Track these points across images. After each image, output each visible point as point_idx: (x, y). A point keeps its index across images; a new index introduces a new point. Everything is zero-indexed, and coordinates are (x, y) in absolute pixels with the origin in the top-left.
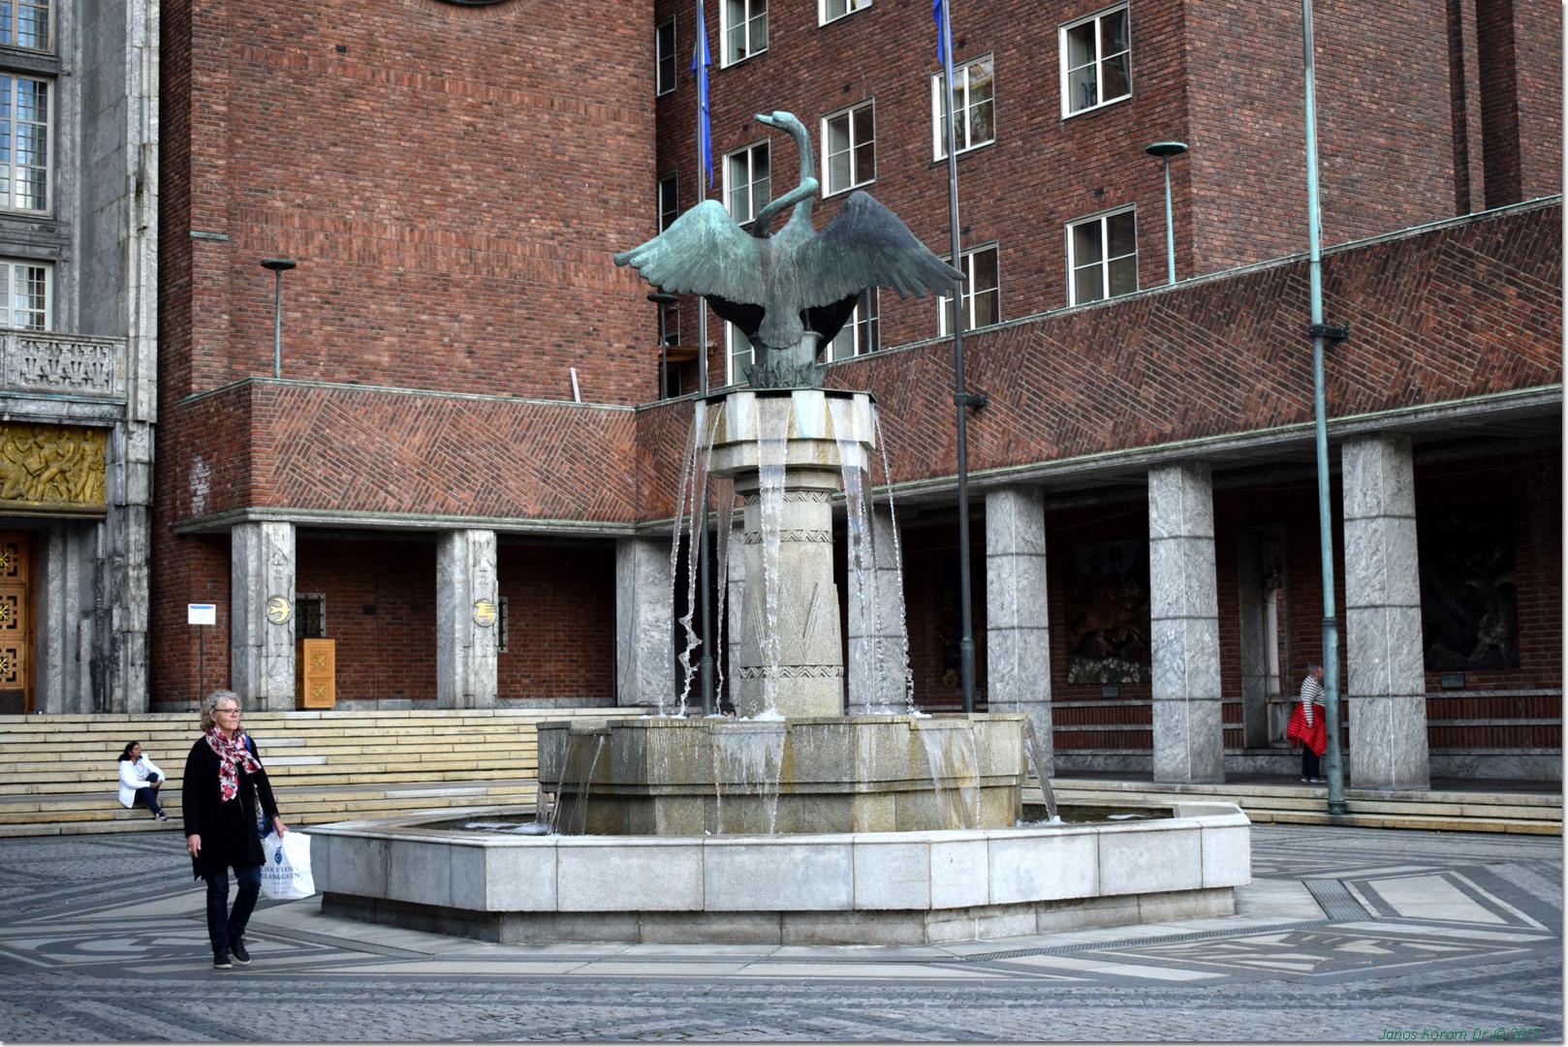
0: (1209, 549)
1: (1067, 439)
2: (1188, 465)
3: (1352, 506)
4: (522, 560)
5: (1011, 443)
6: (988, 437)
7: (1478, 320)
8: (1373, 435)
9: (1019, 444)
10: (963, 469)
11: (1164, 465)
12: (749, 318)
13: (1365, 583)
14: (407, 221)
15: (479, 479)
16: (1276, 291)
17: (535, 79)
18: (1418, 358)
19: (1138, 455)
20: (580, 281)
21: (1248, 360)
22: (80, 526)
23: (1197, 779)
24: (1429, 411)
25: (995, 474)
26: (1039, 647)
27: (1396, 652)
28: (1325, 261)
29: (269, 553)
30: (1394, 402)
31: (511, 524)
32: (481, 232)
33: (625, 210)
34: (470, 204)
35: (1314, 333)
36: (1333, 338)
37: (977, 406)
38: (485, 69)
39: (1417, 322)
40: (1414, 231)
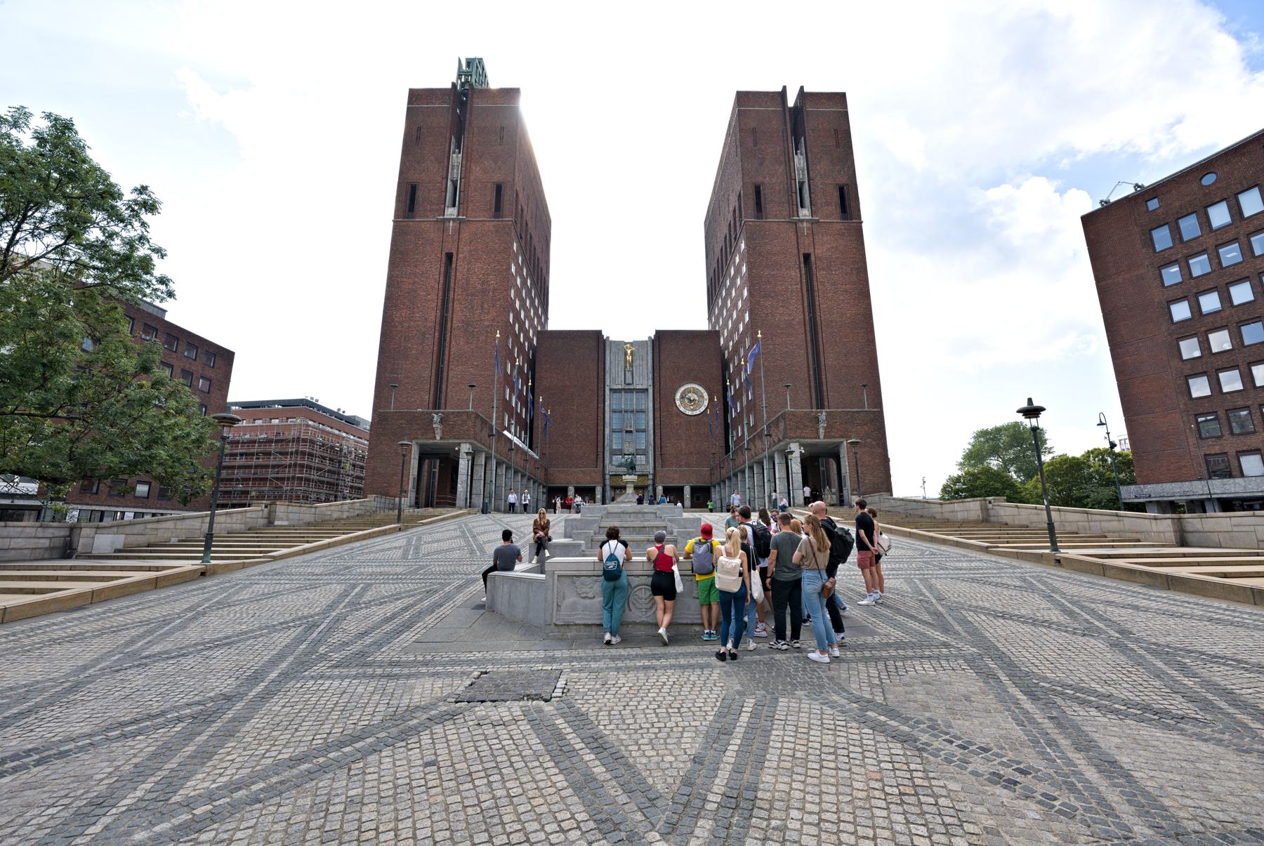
4: (693, 489)
29: (660, 489)
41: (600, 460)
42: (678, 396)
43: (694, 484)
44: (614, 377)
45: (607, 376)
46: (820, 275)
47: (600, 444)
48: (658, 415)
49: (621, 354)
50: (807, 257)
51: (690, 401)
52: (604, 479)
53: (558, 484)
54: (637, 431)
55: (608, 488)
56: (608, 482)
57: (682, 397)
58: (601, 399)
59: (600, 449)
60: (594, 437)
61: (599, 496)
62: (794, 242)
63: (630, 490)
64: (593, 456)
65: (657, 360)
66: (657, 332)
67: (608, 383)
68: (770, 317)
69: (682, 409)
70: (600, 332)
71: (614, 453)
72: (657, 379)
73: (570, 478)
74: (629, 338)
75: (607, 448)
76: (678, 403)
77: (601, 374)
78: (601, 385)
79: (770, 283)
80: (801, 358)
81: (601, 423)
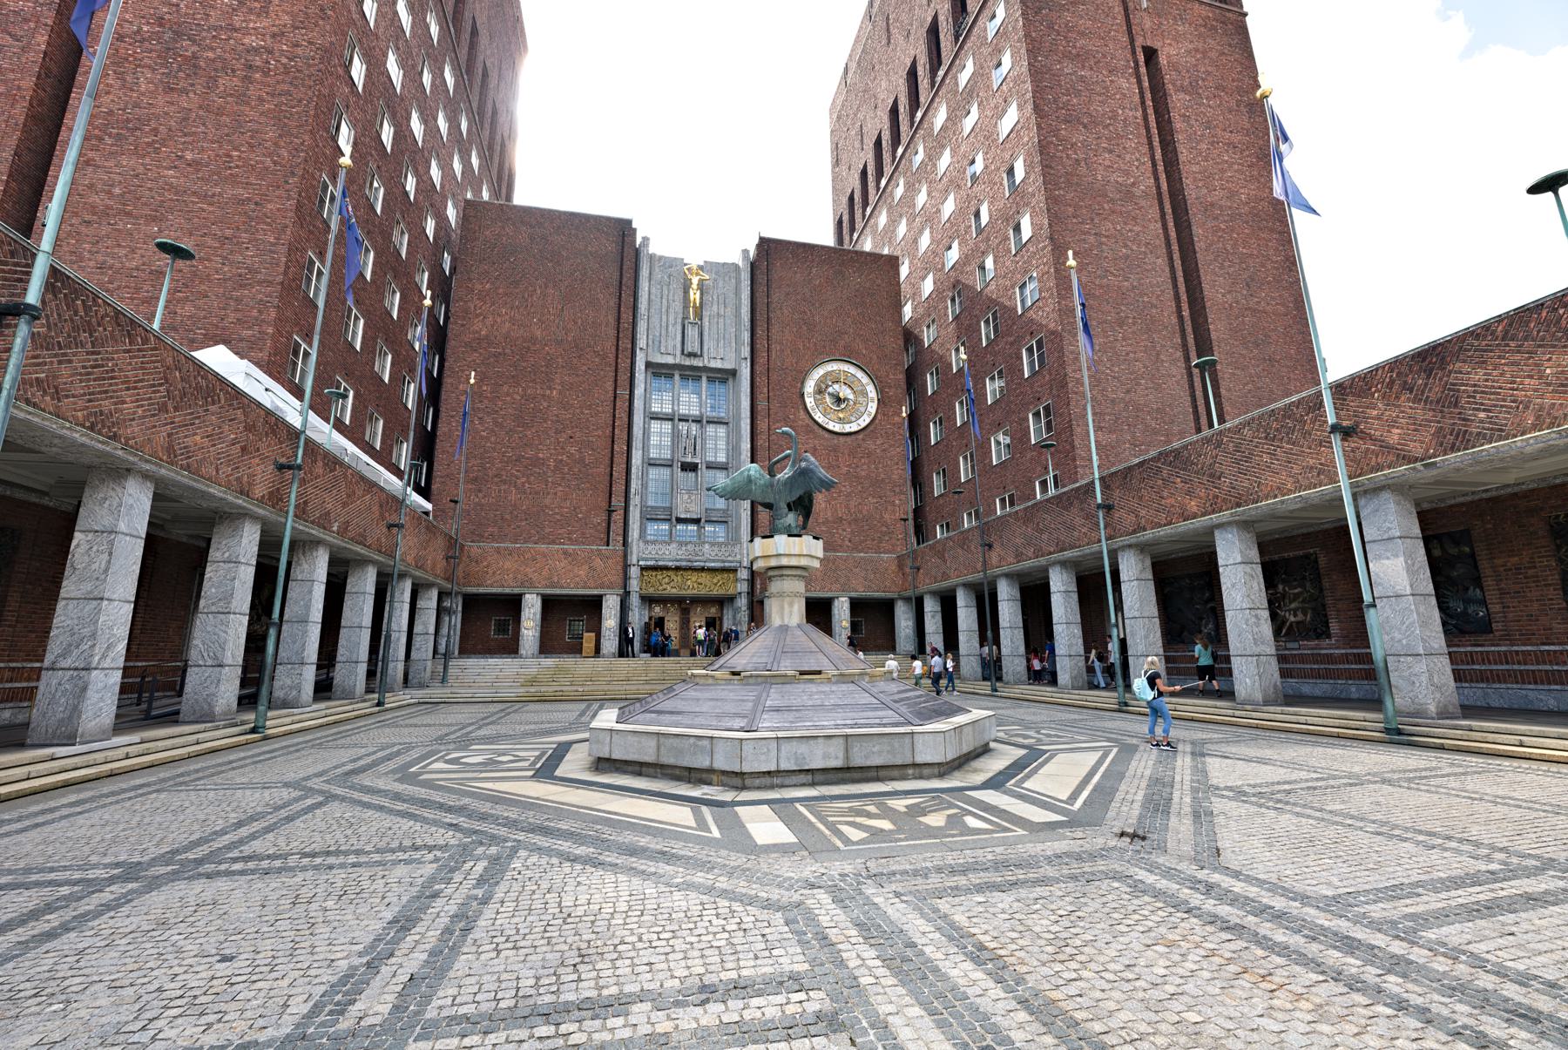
0: (1075, 596)
1: (1019, 557)
2: (1064, 564)
3: (1123, 576)
4: (857, 606)
5: (1001, 559)
6: (994, 557)
7: (1165, 494)
8: (1130, 546)
9: (1003, 561)
10: (984, 571)
11: (1054, 564)
12: (769, 506)
13: (1131, 608)
14: (828, 502)
15: (842, 580)
16: (1086, 492)
17: (869, 455)
18: (1143, 513)
19: (1042, 561)
20: (886, 516)
21: (1078, 521)
22: (731, 599)
23: (1073, 688)
24: (1149, 535)
25: (998, 571)
26: (1019, 635)
27: (1146, 637)
28: (1102, 479)
30: (1134, 532)
31: (854, 594)
32: (852, 503)
33: (902, 493)
34: (849, 495)
35: (1099, 506)
36: (1108, 508)
37: (990, 546)
38: (852, 453)
39: (1141, 498)
40: (1137, 461)
41: (616, 527)
42: (810, 387)
43: (861, 593)
44: (657, 338)
45: (642, 327)
46: (1178, 101)
47: (619, 488)
48: (762, 425)
49: (676, 287)
50: (1151, 54)
51: (838, 400)
52: (626, 578)
53: (491, 587)
54: (710, 466)
55: (635, 600)
56: (634, 585)
57: (820, 391)
58: (623, 378)
59: (617, 502)
60: (603, 469)
61: (610, 622)
62: (1120, 19)
63: (787, 611)
64: (599, 519)
65: (761, 307)
66: (766, 245)
67: (642, 342)
68: (1083, 169)
69: (819, 417)
70: (629, 222)
71: (649, 517)
72: (762, 344)
73: (532, 573)
74: (694, 259)
75: (635, 501)
76: (810, 402)
77: (626, 316)
78: (625, 343)
79: (1078, 93)
80: (1157, 275)
81: (621, 435)
